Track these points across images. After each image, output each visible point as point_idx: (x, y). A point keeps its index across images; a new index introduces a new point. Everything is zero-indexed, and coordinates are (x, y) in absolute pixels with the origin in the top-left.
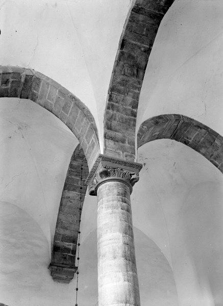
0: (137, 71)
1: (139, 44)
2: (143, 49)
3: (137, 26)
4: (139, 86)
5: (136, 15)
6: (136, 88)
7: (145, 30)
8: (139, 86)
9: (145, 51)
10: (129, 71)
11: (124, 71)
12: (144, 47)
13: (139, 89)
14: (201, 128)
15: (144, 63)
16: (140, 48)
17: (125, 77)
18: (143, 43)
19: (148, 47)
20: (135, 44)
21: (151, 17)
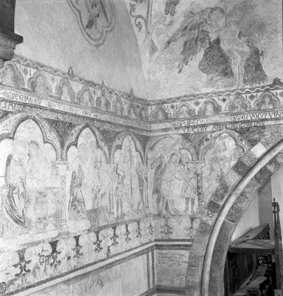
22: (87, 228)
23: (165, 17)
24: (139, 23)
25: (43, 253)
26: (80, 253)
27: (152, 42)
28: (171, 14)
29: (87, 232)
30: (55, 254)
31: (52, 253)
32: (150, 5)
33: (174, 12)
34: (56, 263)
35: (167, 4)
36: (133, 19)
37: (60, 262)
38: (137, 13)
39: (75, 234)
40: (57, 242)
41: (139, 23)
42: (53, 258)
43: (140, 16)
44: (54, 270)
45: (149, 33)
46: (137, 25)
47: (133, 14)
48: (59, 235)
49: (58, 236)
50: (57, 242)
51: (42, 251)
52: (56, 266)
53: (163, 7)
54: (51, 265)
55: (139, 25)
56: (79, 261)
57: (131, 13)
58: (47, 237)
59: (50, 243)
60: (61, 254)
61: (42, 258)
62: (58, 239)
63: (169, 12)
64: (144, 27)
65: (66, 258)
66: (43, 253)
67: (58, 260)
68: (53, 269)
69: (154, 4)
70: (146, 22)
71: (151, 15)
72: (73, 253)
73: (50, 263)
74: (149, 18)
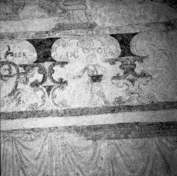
22: (163, 19)
25: (10, 58)
26: (138, 70)
29: (162, 27)
30: (47, 65)
31: (37, 62)
34: (49, 82)
37: (62, 83)
39: (117, 29)
40: (53, 40)
42: (41, 71)
44: (43, 97)
48: (60, 28)
49: (54, 30)
50: (53, 40)
51: (7, 53)
52: (49, 89)
54: (35, 84)
56: (132, 89)
58: (22, 29)
59: (32, 41)
60: (66, 66)
61: (6, 67)
62: (57, 35)
65: (86, 78)
66: (10, 58)
67: (56, 76)
68: (40, 93)
72: (109, 71)
73: (31, 80)
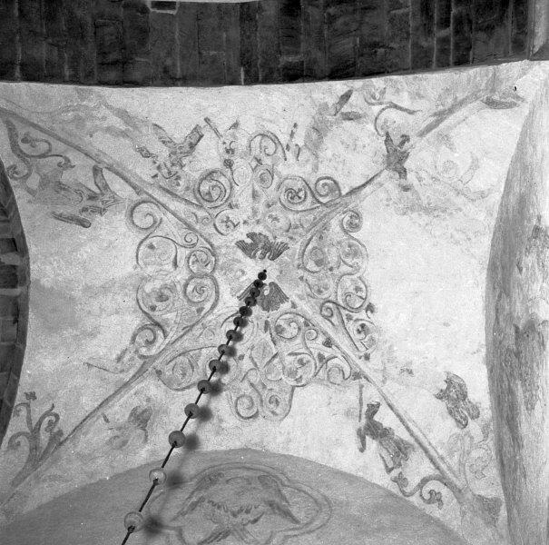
0: (115, 63)
1: (178, 50)
2: (169, 62)
3: (213, 29)
4: (82, 74)
5: (234, 19)
6: (74, 68)
7: (212, 53)
8: (82, 74)
9: (166, 71)
10: (107, 38)
11: (104, 25)
12: (174, 65)
13: (75, 80)
14: (16, 321)
15: (137, 75)
16: (169, 54)
17: (90, 29)
18: (183, 58)
19: (179, 74)
20: (173, 40)
21: (242, 55)
23: (468, 434)
24: (431, 492)
27: (481, 498)
28: (472, 418)
32: (426, 444)
33: (476, 408)
35: (450, 413)
36: (415, 500)
38: (414, 480)
41: (431, 492)
43: (425, 481)
45: (460, 491)
46: (429, 502)
47: (408, 490)
53: (450, 422)
55: (435, 498)
57: (403, 492)
63: (465, 419)
64: (445, 491)
69: (431, 436)
70: (442, 478)
71: (442, 458)
74: (443, 466)
